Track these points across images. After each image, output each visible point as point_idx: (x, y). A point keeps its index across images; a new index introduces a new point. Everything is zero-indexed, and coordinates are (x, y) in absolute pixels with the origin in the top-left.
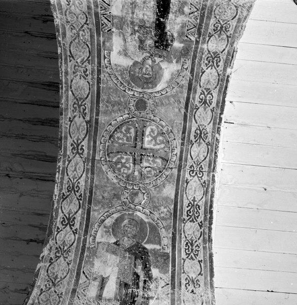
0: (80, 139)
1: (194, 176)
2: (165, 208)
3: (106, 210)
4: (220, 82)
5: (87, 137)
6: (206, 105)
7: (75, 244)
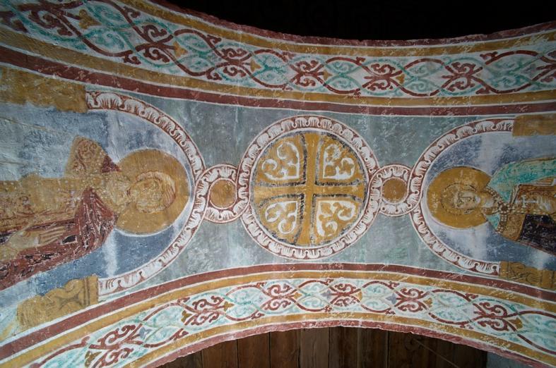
0: (325, 78)
1: (269, 294)
2: (206, 255)
3: (192, 135)
4: (445, 324)
5: (330, 92)
6: (398, 301)
7: (88, 51)
